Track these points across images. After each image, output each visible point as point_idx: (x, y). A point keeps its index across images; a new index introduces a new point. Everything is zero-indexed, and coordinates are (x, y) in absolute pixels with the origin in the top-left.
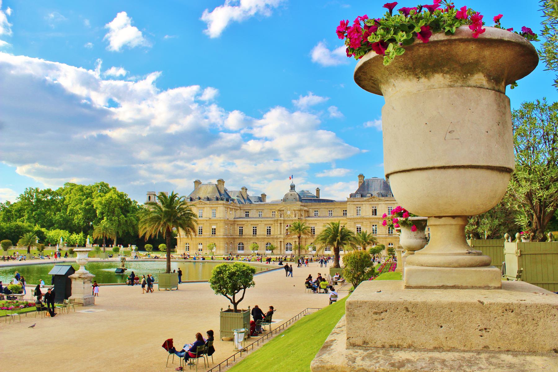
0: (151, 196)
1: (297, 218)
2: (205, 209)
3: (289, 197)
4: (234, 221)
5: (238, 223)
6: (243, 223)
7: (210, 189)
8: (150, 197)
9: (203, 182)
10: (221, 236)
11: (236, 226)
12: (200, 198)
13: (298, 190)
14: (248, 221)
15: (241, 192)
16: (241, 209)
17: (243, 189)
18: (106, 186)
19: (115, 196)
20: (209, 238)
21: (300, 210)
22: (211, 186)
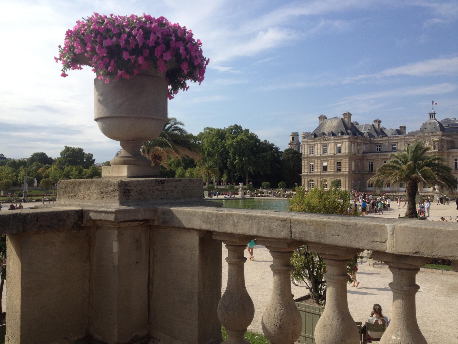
0: (294, 136)
1: (436, 150)
2: (330, 145)
3: (429, 127)
4: (363, 156)
5: (368, 158)
6: (373, 158)
7: (335, 123)
8: (293, 138)
9: (328, 116)
10: (347, 173)
11: (365, 162)
12: (324, 134)
13: (440, 118)
14: (378, 156)
15: (373, 125)
16: (371, 143)
17: (375, 121)
18: (240, 128)
19: (244, 137)
20: (333, 175)
21: (441, 141)
22: (337, 121)
